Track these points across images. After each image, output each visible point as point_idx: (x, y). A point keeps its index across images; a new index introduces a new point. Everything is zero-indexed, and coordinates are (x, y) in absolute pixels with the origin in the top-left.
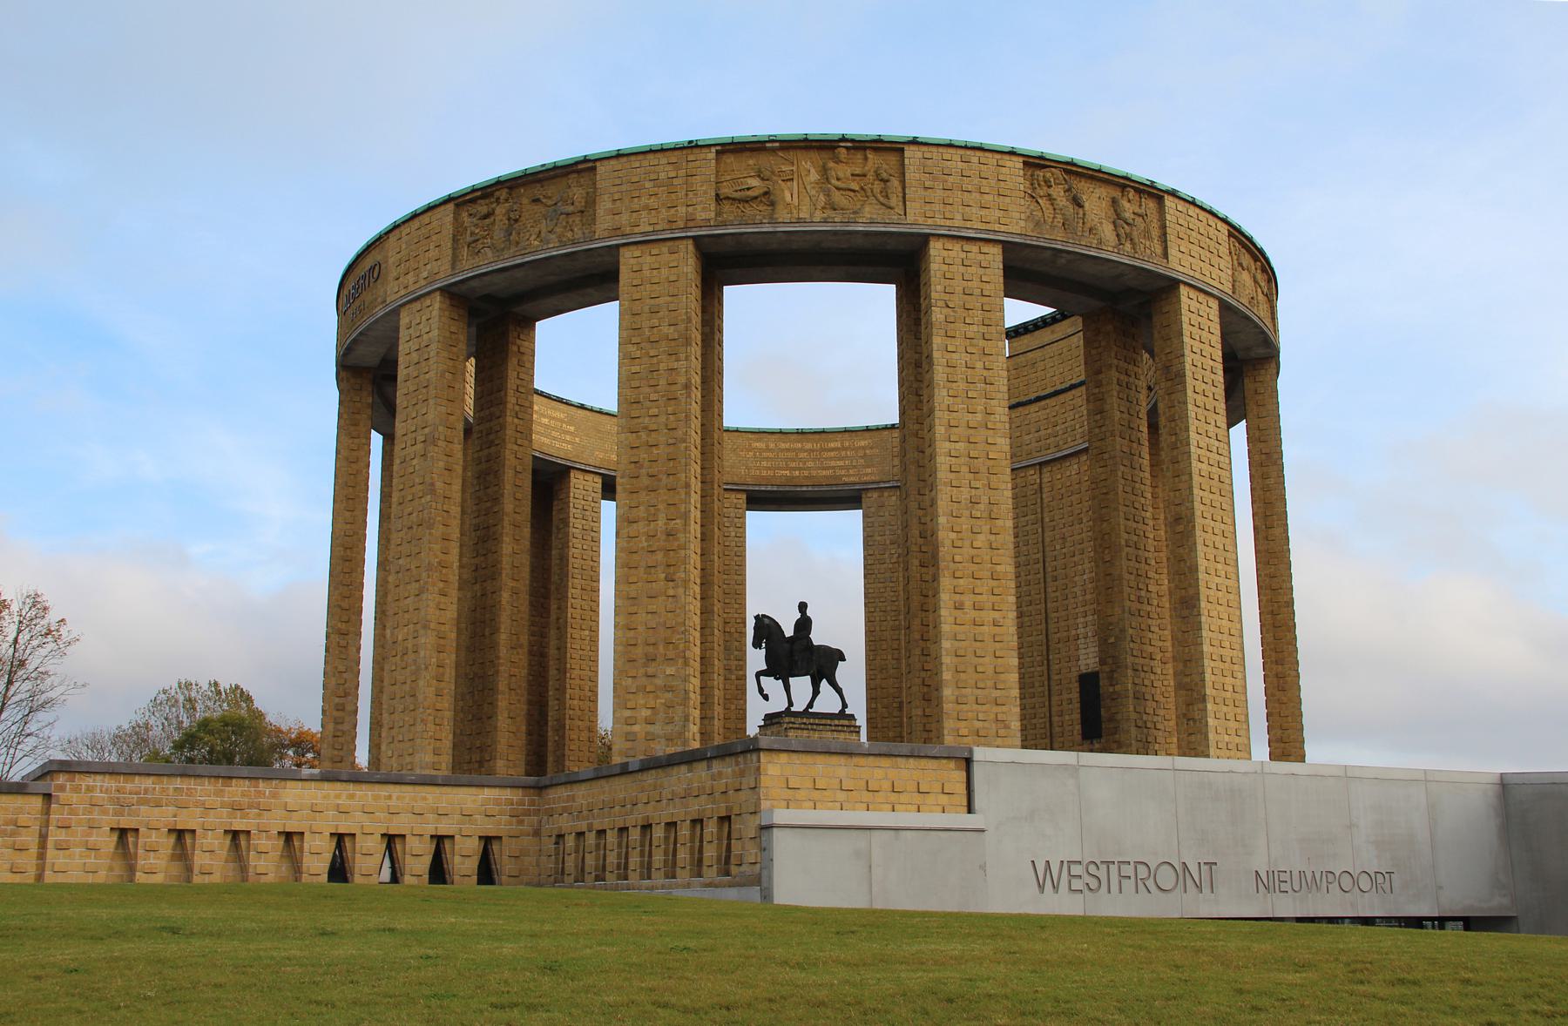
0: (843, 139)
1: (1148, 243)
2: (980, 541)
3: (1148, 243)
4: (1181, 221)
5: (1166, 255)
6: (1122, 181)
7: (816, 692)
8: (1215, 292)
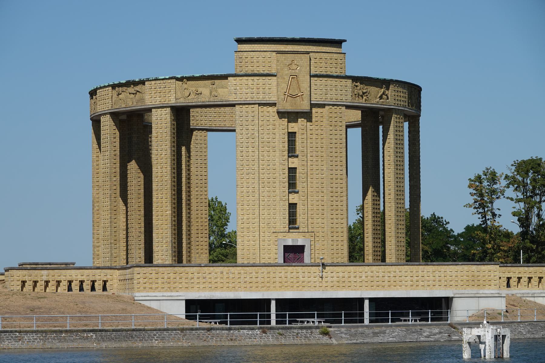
8: (107, 112)
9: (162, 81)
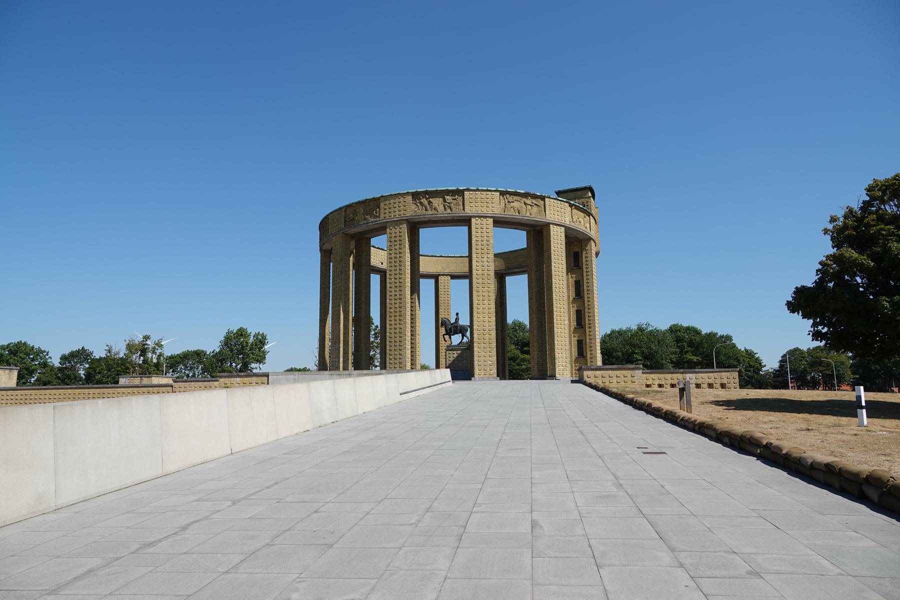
0: (366, 200)
1: (457, 207)
3: (457, 207)
5: (464, 210)
7: (463, 339)
8: (489, 215)
9: (559, 202)
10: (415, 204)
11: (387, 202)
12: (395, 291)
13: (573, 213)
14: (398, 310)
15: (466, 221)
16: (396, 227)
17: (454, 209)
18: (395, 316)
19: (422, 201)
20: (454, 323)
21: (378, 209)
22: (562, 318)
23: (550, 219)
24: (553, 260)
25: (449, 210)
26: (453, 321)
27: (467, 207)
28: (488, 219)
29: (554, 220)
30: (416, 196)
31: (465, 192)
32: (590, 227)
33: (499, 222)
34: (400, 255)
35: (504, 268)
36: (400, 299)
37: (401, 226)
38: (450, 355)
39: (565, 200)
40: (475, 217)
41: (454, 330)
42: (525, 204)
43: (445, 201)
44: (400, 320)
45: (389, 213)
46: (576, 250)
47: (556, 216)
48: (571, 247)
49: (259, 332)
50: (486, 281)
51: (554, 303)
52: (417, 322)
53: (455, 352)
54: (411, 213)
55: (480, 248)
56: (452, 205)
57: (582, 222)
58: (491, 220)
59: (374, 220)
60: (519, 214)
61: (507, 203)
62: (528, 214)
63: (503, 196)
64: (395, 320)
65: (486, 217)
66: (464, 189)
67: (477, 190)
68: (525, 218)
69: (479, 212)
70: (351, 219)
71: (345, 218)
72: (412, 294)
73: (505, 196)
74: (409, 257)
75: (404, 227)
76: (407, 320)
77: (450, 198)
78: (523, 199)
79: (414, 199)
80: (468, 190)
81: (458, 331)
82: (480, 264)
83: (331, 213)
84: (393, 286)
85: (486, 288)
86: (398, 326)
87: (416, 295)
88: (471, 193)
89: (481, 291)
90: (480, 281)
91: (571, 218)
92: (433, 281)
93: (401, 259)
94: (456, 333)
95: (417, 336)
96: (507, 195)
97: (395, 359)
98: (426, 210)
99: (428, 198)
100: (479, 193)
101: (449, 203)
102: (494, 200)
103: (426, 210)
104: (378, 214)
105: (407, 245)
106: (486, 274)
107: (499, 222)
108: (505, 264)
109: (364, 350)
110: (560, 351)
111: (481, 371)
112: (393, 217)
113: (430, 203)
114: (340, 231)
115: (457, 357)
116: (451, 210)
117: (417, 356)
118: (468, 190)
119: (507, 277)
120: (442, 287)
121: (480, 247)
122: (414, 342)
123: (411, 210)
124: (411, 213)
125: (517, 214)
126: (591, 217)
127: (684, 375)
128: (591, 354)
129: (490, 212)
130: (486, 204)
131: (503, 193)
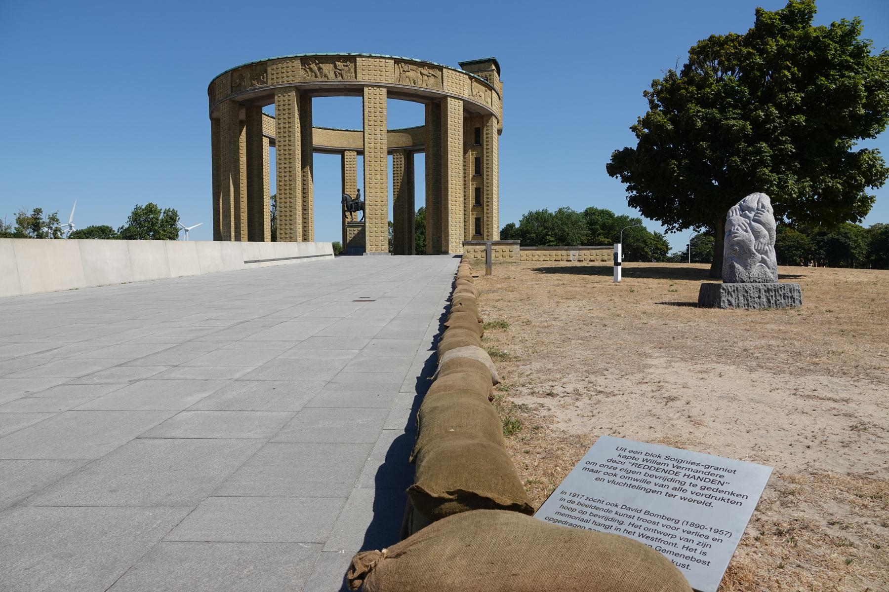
0: (253, 63)
1: (349, 75)
2: (287, 179)
4: (364, 64)
5: (356, 78)
6: (336, 56)
8: (383, 85)
9: (458, 74)
10: (304, 69)
11: (275, 67)
12: (285, 163)
13: (473, 86)
14: (288, 183)
15: (358, 90)
16: (284, 95)
17: (345, 77)
18: (285, 190)
19: (311, 66)
20: (355, 199)
21: (265, 74)
22: (457, 195)
23: (448, 91)
24: (449, 135)
25: (340, 77)
26: (354, 197)
27: (359, 75)
28: (381, 89)
29: (452, 92)
30: (305, 60)
31: (357, 59)
32: (492, 102)
33: (394, 93)
34: (289, 125)
35: (411, 145)
36: (290, 172)
37: (289, 94)
38: (351, 232)
39: (464, 72)
40: (367, 86)
41: (355, 206)
42: (422, 74)
43: (335, 67)
44: (290, 194)
45: (277, 78)
46: (478, 126)
47: (454, 88)
48: (473, 123)
49: (170, 209)
50: (379, 154)
51: (449, 179)
52: (310, 196)
53: (356, 229)
54: (300, 79)
55: (372, 120)
56: (343, 72)
57: (483, 97)
58: (385, 90)
59: (261, 86)
60: (415, 84)
61: (402, 72)
62: (424, 85)
63: (398, 65)
64: (285, 194)
65: (379, 87)
66: (356, 55)
67: (370, 57)
68: (420, 89)
69: (372, 81)
70: (237, 84)
71: (231, 83)
72: (303, 168)
73: (400, 65)
74: (300, 127)
75: (293, 94)
76: (297, 194)
77: (342, 64)
78: (420, 69)
79: (303, 64)
80: (360, 56)
81: (359, 208)
82: (372, 137)
83: (217, 77)
84: (283, 158)
85: (378, 163)
86: (288, 200)
87: (308, 169)
88: (364, 59)
89: (373, 165)
90: (373, 154)
91: (470, 91)
92: (340, 156)
93: (290, 130)
94: (357, 209)
95: (310, 210)
96: (403, 64)
97: (286, 234)
98: (316, 77)
99: (318, 64)
100: (373, 60)
101: (340, 70)
102: (388, 68)
103: (316, 77)
104: (265, 80)
105: (296, 114)
106: (379, 148)
107: (394, 93)
108: (413, 140)
109: (257, 225)
110: (454, 228)
111: (373, 247)
112: (280, 83)
113: (320, 69)
114: (227, 97)
115: (358, 233)
116: (342, 77)
117: (310, 231)
118: (360, 56)
119: (415, 154)
120: (347, 163)
121: (372, 118)
122: (307, 217)
123: (300, 75)
124: (300, 79)
125: (413, 85)
126: (493, 91)
127: (568, 252)
128: (488, 232)
129: (383, 81)
130: (379, 72)
131: (397, 61)
